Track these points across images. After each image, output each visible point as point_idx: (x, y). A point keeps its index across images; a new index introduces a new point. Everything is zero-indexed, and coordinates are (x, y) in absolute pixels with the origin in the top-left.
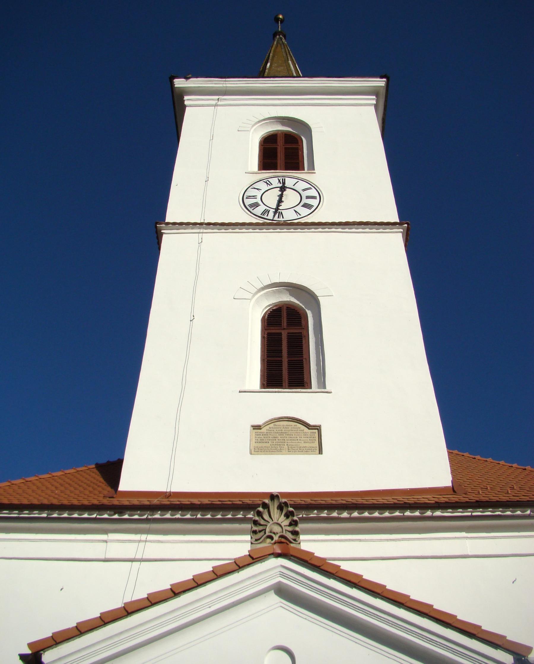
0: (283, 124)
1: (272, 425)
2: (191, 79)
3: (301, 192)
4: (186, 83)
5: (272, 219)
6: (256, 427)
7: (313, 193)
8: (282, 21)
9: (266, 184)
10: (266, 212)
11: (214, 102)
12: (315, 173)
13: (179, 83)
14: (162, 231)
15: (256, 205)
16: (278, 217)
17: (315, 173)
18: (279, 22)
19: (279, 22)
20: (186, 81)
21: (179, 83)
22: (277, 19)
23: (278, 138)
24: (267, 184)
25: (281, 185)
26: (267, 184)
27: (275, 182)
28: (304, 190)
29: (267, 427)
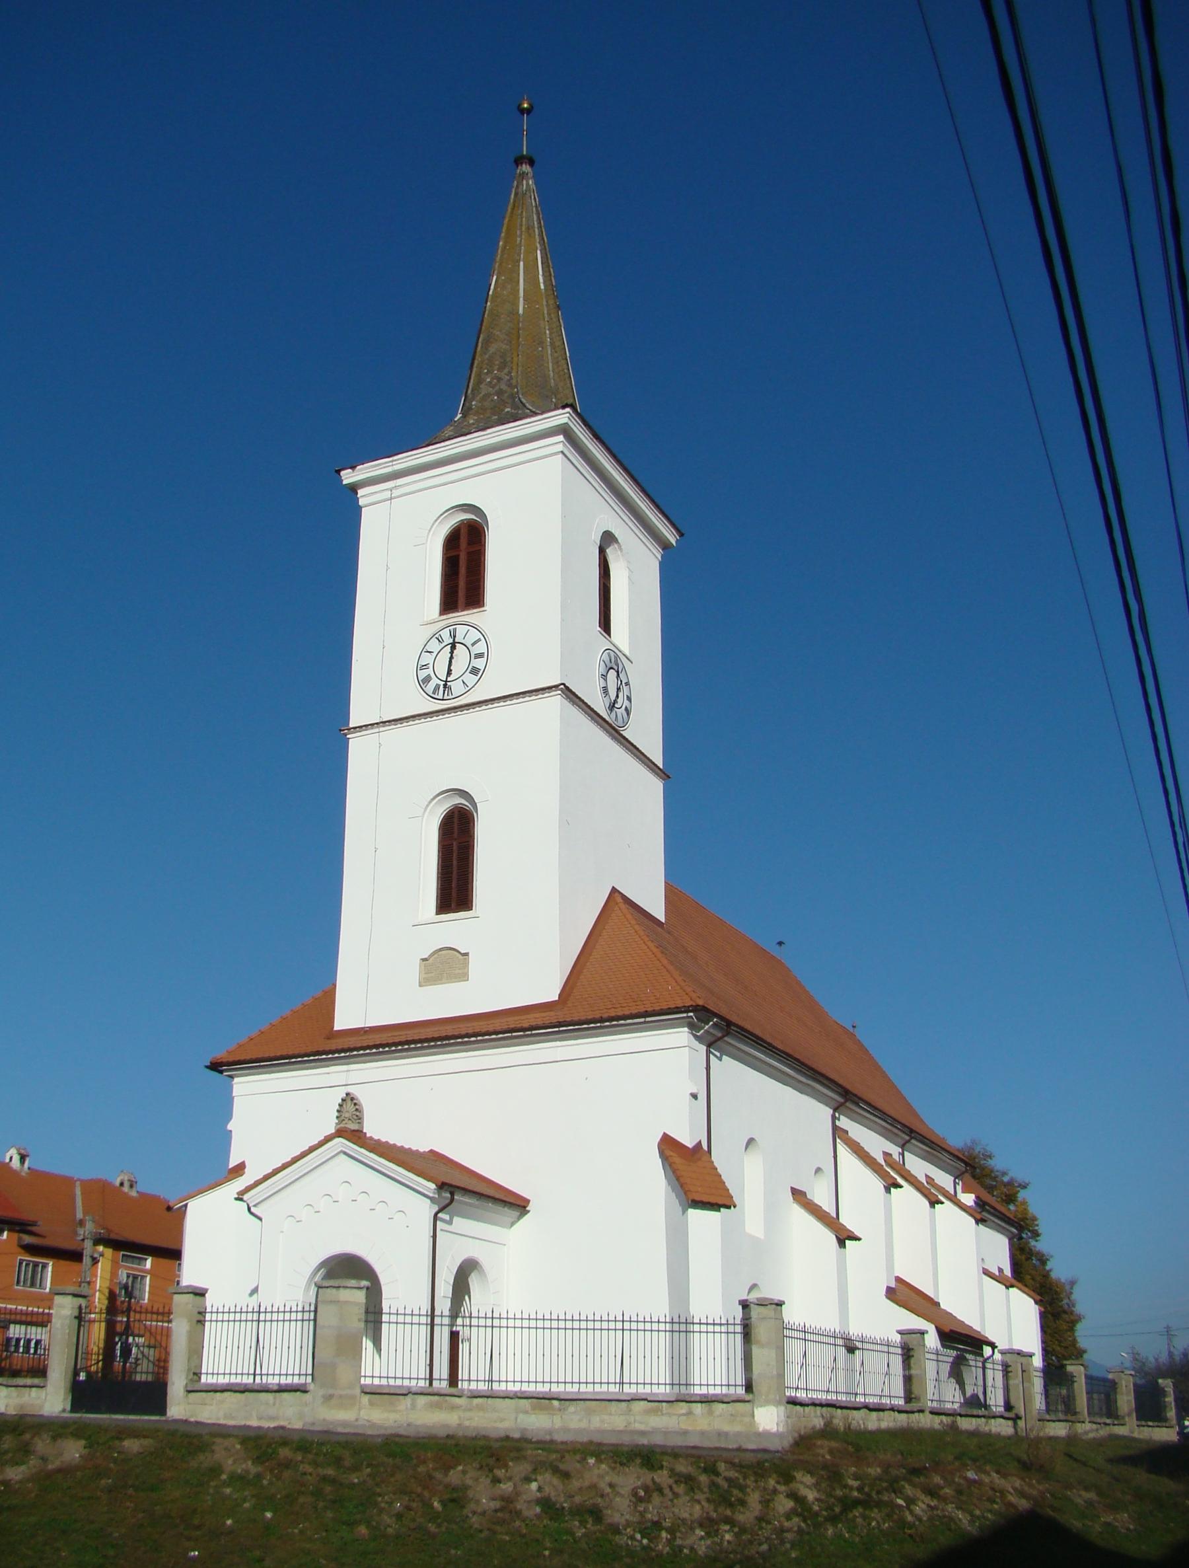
0: (465, 511)
1: (436, 956)
2: (358, 467)
3: (470, 647)
4: (355, 474)
5: (441, 698)
6: (424, 960)
7: (481, 648)
8: (529, 111)
9: (438, 641)
10: (438, 687)
11: (387, 494)
12: (485, 611)
13: (348, 477)
14: (348, 736)
15: (427, 679)
16: (448, 695)
17: (485, 611)
18: (525, 115)
19: (525, 115)
20: (353, 471)
21: (348, 477)
22: (522, 111)
23: (462, 531)
24: (439, 641)
25: (451, 641)
26: (439, 641)
27: (445, 634)
28: (473, 644)
29: (433, 958)
